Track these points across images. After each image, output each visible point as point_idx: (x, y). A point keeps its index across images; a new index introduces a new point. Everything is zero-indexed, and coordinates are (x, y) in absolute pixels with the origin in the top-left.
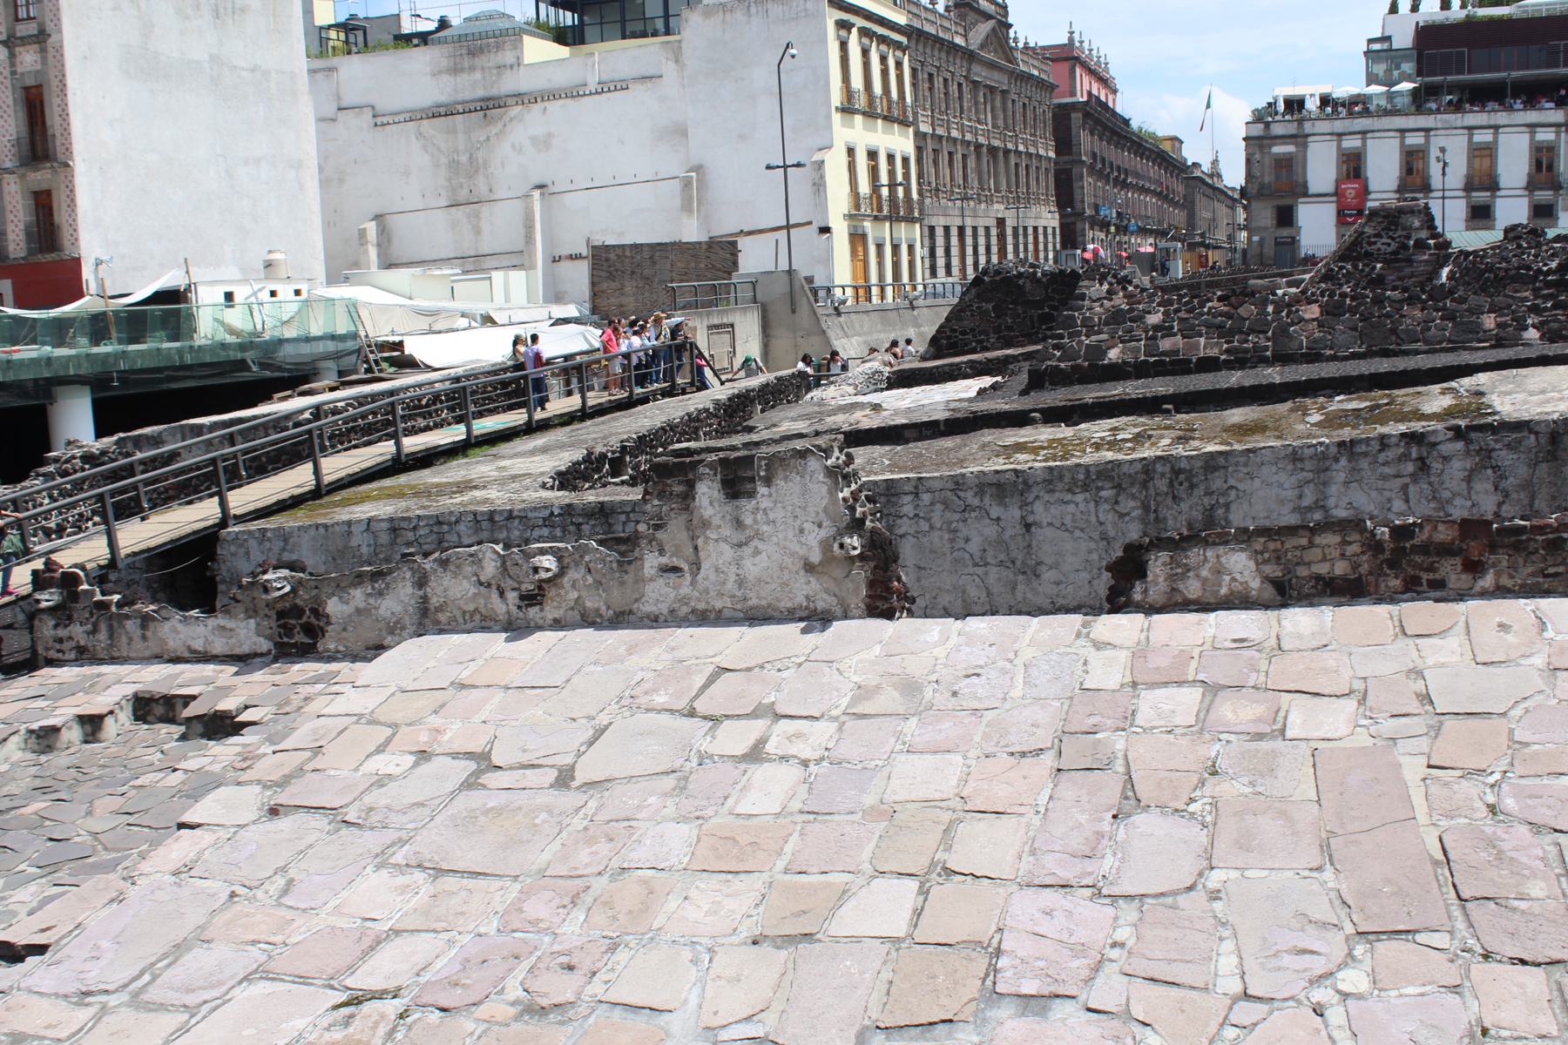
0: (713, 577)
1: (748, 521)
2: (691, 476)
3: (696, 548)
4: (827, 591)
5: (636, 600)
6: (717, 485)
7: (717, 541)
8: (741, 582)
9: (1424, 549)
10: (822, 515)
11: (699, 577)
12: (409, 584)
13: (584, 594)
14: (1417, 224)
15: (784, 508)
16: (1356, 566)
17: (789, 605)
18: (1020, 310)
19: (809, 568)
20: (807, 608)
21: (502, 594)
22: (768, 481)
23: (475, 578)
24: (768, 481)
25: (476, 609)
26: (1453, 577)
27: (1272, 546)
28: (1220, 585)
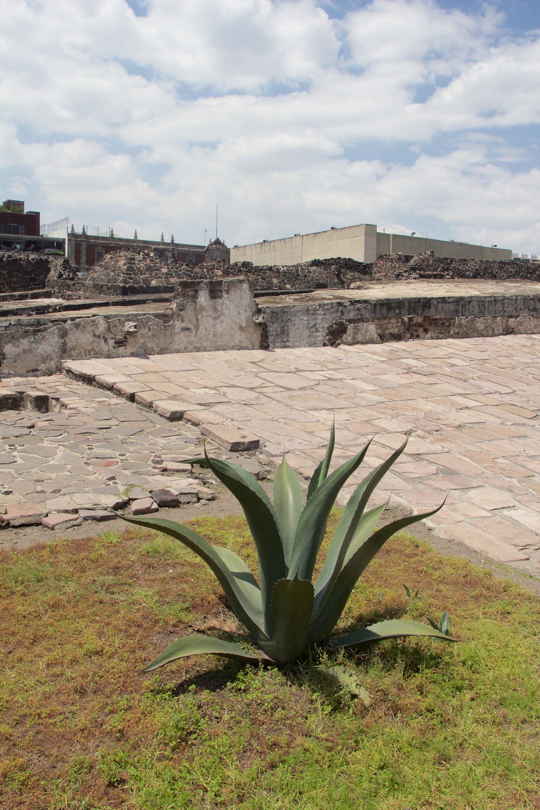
0: (204, 332)
1: (219, 308)
2: (197, 288)
3: (197, 320)
4: (247, 338)
5: (170, 343)
6: (208, 292)
7: (207, 316)
8: (215, 335)
9: (415, 325)
10: (247, 307)
11: (199, 332)
12: (56, 336)
13: (147, 340)
14: (170, 255)
15: (233, 303)
16: (400, 330)
17: (233, 344)
18: (20, 275)
19: (241, 329)
20: (239, 345)
21: (106, 341)
22: (228, 292)
23: (93, 333)
24: (228, 292)
25: (92, 349)
26: (421, 334)
27: (380, 323)
28: (366, 336)
